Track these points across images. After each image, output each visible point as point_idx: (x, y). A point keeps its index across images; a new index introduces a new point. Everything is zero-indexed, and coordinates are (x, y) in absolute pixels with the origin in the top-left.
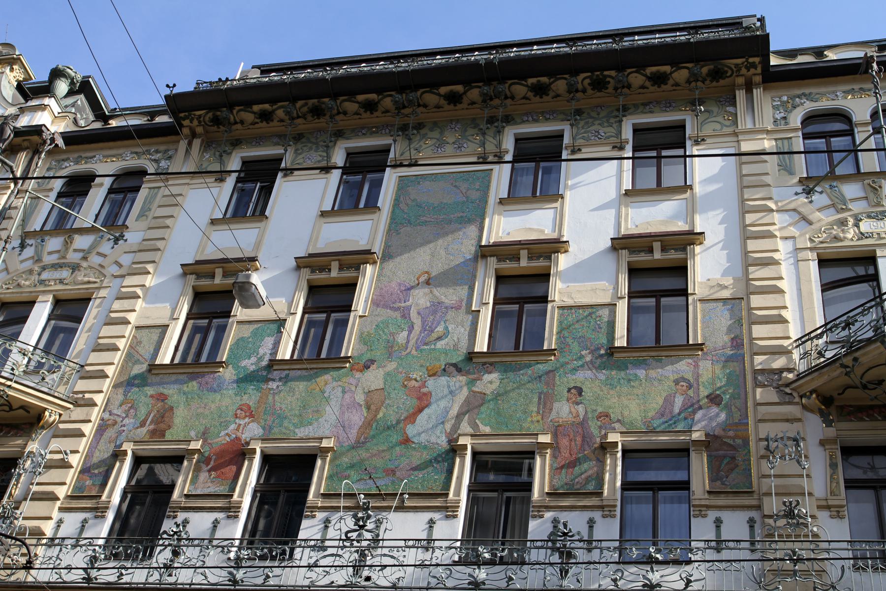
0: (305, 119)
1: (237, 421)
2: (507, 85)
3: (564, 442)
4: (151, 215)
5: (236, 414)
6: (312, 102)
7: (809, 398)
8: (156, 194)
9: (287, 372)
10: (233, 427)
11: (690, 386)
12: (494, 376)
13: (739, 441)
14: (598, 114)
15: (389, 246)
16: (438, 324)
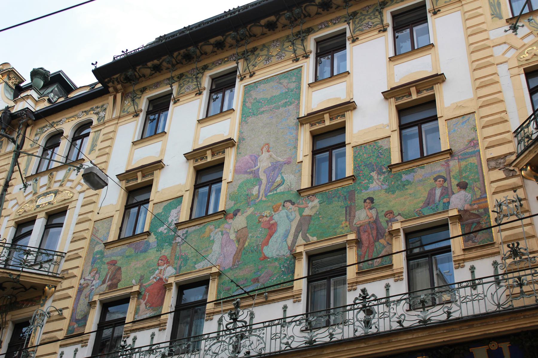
0: (182, 64)
1: (160, 268)
2: (303, 8)
4: (97, 148)
5: (158, 264)
6: (182, 51)
7: (526, 170)
8: (99, 134)
9: (186, 229)
10: (157, 272)
11: (445, 180)
12: (316, 201)
13: (482, 211)
14: (367, 12)
15: (242, 133)
16: (277, 176)
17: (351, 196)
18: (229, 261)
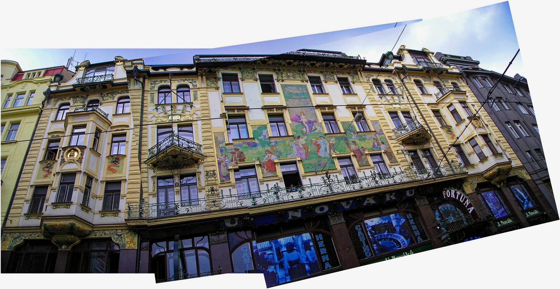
3: (357, 154)
12: (333, 139)
17: (346, 139)
18: (304, 156)
